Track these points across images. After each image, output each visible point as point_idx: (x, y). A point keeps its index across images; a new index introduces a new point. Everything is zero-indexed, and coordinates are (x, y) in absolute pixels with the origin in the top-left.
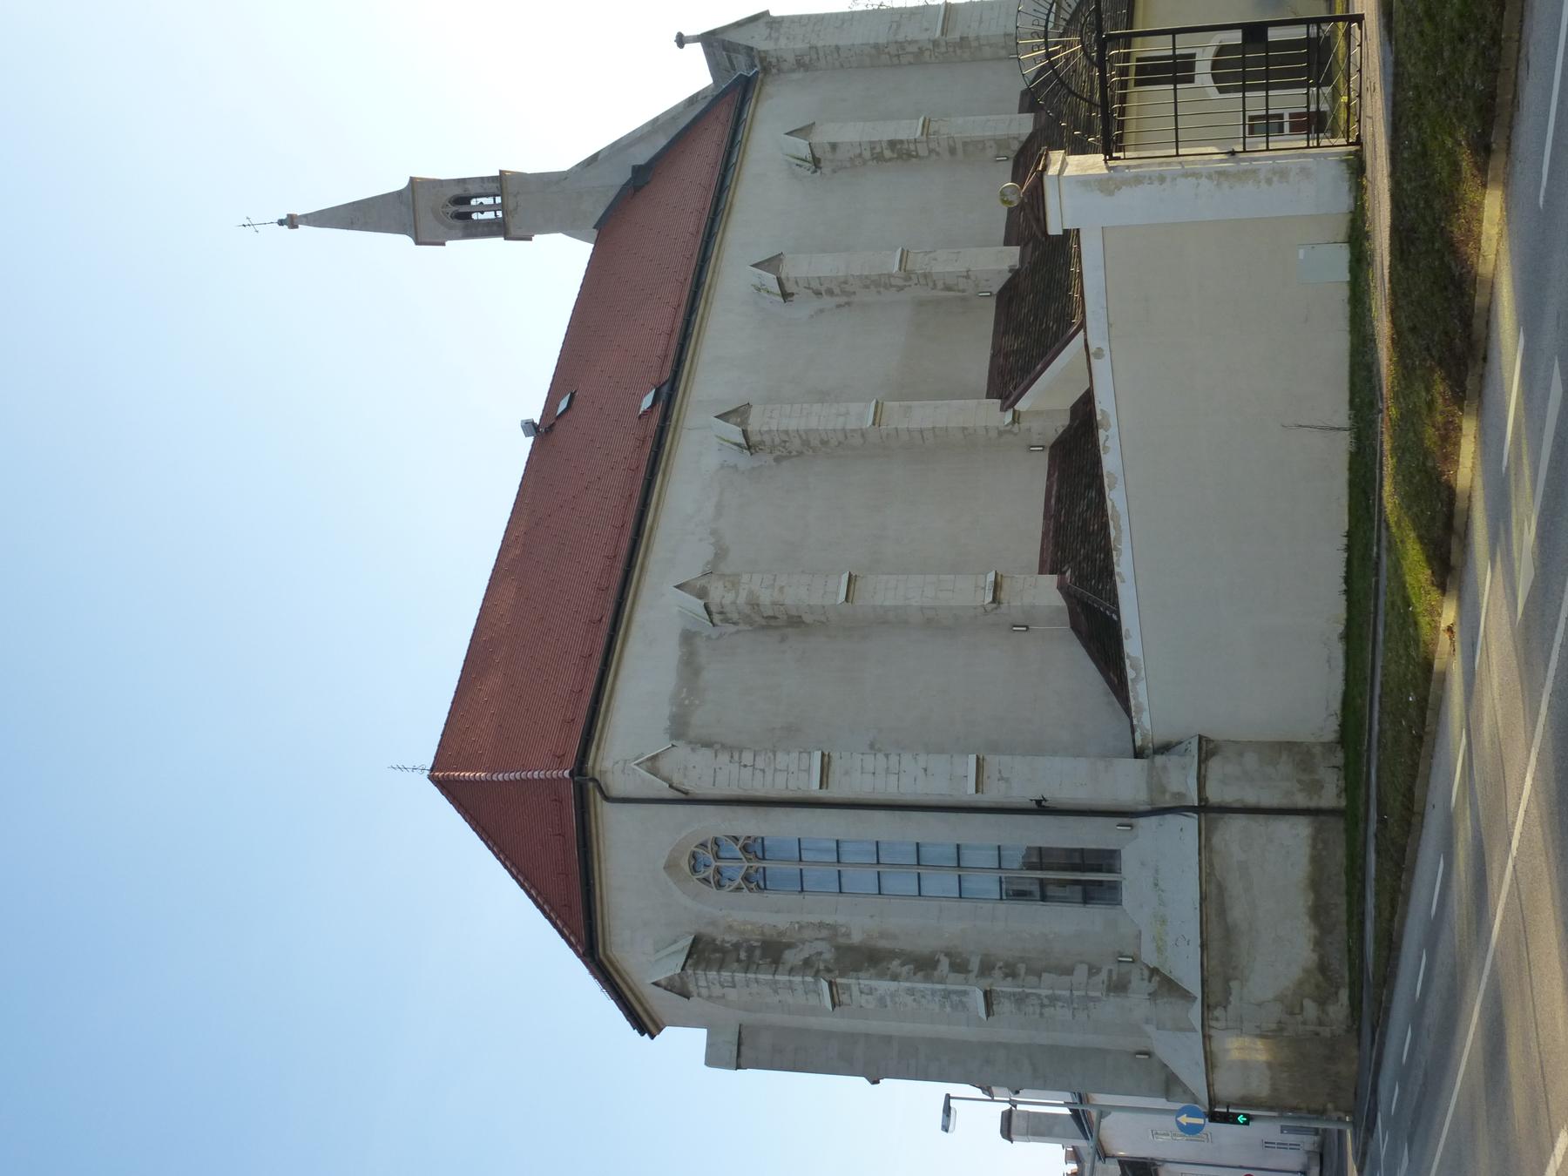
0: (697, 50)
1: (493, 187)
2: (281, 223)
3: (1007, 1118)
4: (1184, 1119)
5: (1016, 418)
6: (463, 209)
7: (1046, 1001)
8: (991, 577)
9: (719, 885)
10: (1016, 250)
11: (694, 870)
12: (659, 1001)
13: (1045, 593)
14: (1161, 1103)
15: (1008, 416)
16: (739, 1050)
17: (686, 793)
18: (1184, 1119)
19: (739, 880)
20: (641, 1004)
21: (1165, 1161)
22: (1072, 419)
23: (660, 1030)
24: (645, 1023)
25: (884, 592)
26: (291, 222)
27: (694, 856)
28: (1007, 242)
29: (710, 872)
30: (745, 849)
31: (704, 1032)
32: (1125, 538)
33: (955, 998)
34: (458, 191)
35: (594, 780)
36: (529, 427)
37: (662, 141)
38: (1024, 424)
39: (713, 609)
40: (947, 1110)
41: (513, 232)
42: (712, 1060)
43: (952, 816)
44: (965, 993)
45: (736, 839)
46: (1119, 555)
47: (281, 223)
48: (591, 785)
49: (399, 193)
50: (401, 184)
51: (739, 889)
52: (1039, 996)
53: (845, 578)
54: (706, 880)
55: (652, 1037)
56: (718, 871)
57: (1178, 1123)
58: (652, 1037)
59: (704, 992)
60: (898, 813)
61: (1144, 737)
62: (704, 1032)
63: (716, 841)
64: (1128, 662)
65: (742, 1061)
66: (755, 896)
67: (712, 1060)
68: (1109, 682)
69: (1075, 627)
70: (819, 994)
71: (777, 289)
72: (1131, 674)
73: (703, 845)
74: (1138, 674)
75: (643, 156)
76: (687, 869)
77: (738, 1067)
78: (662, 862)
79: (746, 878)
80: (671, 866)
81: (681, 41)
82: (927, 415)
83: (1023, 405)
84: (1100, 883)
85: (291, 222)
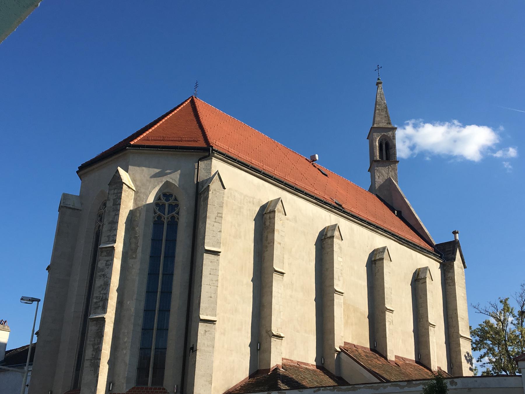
6: (384, 146)
7: (96, 347)
10: (393, 359)
11: (165, 195)
13: (276, 360)
15: (339, 350)
17: (201, 194)
20: (97, 168)
24: (84, 169)
27: (171, 195)
28: (396, 356)
30: (173, 217)
33: (101, 304)
34: (391, 144)
37: (412, 223)
39: (272, 215)
40: (33, 300)
42: (65, 197)
43: (185, 309)
45: (178, 213)
47: (378, 79)
48: (207, 154)
51: (155, 213)
55: (77, 172)
58: (77, 172)
59: (112, 191)
63: (177, 205)
67: (65, 197)
71: (377, 258)
73: (176, 199)
75: (404, 214)
77: (60, 207)
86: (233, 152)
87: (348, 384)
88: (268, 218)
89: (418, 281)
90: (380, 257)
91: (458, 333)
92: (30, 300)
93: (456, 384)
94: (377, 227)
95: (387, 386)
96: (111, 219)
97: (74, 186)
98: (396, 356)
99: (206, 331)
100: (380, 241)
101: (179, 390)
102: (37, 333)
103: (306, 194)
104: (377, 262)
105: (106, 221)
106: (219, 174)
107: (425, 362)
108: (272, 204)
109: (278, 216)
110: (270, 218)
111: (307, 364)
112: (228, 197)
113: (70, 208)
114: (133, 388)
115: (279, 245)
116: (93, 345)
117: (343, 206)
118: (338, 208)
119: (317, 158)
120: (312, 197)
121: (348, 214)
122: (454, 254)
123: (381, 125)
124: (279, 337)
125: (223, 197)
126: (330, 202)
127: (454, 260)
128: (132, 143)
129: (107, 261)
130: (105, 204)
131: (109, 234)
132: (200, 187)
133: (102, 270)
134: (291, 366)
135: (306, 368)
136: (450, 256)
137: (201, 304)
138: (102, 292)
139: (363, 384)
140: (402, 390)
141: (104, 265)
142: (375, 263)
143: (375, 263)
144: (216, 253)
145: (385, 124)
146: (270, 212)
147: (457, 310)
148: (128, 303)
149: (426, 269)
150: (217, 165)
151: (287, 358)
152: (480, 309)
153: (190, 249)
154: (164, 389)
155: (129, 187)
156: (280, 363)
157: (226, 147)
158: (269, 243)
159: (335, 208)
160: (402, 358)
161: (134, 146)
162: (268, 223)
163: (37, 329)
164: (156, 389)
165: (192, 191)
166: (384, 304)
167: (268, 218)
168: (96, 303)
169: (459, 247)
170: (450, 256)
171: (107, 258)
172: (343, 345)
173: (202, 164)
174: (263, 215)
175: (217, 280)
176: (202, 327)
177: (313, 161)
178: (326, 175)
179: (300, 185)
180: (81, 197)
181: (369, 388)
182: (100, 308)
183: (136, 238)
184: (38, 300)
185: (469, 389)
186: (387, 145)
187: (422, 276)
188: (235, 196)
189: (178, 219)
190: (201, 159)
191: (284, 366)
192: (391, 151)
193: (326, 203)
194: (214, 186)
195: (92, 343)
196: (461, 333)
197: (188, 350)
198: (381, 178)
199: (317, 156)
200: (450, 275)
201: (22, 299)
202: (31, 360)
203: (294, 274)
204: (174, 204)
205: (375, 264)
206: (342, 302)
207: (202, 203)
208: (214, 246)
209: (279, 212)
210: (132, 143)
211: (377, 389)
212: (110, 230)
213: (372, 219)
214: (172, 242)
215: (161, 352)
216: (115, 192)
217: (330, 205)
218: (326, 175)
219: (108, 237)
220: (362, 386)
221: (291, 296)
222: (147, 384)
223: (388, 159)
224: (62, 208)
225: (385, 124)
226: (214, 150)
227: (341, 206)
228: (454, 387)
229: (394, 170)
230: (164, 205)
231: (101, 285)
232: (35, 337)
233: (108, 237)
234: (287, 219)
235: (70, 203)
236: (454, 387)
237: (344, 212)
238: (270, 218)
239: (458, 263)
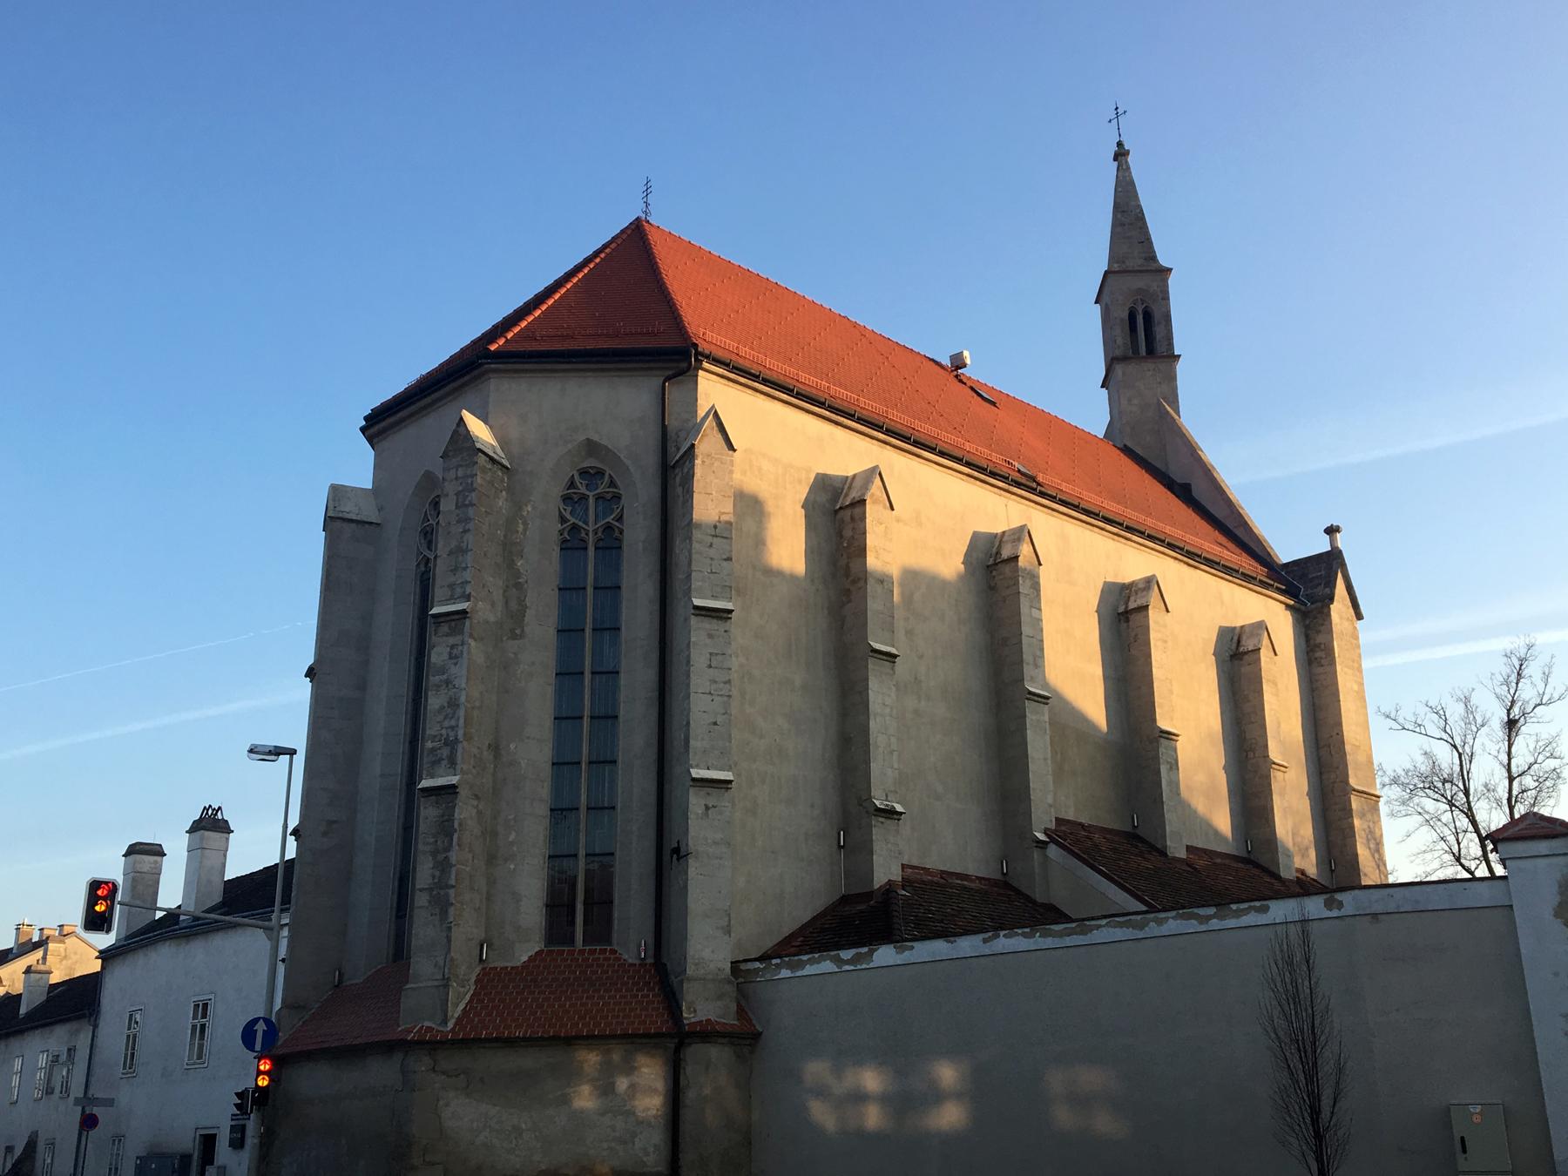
0: (1323, 546)
1: (1160, 348)
2: (1120, 144)
3: (157, 851)
4: (261, 1027)
5: (1042, 845)
7: (441, 857)
8: (899, 808)
9: (566, 499)
10: (1182, 854)
11: (584, 473)
12: (428, 432)
13: (885, 870)
14: (278, 1004)
15: (1041, 836)
16: (344, 525)
17: (673, 467)
18: (261, 1027)
19: (573, 520)
20: (411, 415)
21: (95, 1026)
22: (1043, 905)
23: (370, 440)
24: (379, 424)
25: (881, 694)
26: (1121, 154)
27: (601, 473)
29: (583, 490)
30: (608, 528)
31: (370, 487)
32: (1049, 942)
33: (445, 752)
34: (1157, 316)
35: (689, 368)
36: (958, 363)
38: (1036, 854)
39: (857, 510)
40: (278, 752)
41: (1119, 369)
42: (337, 493)
44: (452, 763)
45: (620, 519)
46: (1025, 935)
47: (1120, 144)
48: (685, 365)
49: (1154, 258)
50: (1164, 261)
51: (563, 520)
52: (448, 849)
53: (894, 651)
54: (572, 484)
55: (363, 430)
56: (584, 498)
57: (255, 1021)
58: (363, 430)
59: (452, 474)
60: (656, 694)
61: (757, 971)
62: (370, 487)
63: (617, 497)
64: (865, 950)
65: (338, 524)
66: (554, 537)
67: (337, 493)
68: (792, 936)
69: (844, 900)
70: (452, 599)
71: (1132, 605)
72: (846, 954)
73: (612, 484)
74: (848, 962)
76: (585, 465)
78: (596, 438)
79: (575, 528)
80: (592, 447)
81: (1331, 531)
82: (1038, 747)
83: (1053, 851)
84: (572, 923)
85: (1121, 154)
86: (748, 354)
87: (1069, 920)
88: (847, 518)
89: (1237, 656)
90: (1140, 602)
91: (1347, 783)
92: (270, 753)
93: (1340, 905)
94: (1129, 529)
95: (1167, 919)
96: (454, 544)
97: (357, 466)
98: (1188, 847)
99: (707, 808)
100: (1135, 562)
101: (651, 952)
102: (295, 832)
103: (942, 454)
104: (1132, 617)
105: (442, 547)
106: (716, 415)
107: (1264, 860)
108: (857, 484)
109: (874, 513)
110: (852, 519)
111: (965, 877)
112: (744, 473)
113: (351, 521)
114: (539, 953)
115: (879, 588)
116: (434, 854)
117: (1040, 479)
118: (1027, 485)
119: (968, 361)
120: (958, 460)
121: (1052, 498)
122: (1331, 584)
123: (1130, 264)
124: (890, 813)
125: (731, 472)
126: (1004, 471)
127: (1331, 599)
128: (493, 347)
129: (452, 647)
130: (436, 504)
131: (452, 579)
132: (671, 449)
133: (442, 671)
134: (923, 882)
135: (965, 888)
136: (1321, 591)
137: (692, 742)
138: (446, 724)
139: (1105, 917)
140: (1203, 928)
141: (446, 656)
142: (1125, 616)
143: (1125, 616)
144: (722, 615)
145: (1140, 262)
146: (853, 505)
147: (1340, 724)
148: (512, 746)
149: (1261, 626)
150: (712, 390)
151: (915, 862)
152: (1401, 720)
153: (657, 607)
154: (613, 952)
155: (491, 459)
156: (896, 875)
157: (732, 344)
158: (854, 582)
159: (1018, 485)
160: (1205, 851)
161: (500, 356)
162: (848, 533)
163: (294, 822)
164: (592, 952)
165: (651, 461)
166: (1154, 720)
167: (847, 518)
168: (433, 750)
169: (1343, 565)
170: (1321, 591)
171: (452, 640)
172: (1053, 826)
173: (674, 393)
174: (836, 512)
175: (729, 682)
176: (696, 802)
177: (958, 368)
178: (994, 404)
179: (925, 429)
180: (376, 490)
181: (1121, 925)
182: (444, 762)
183: (518, 586)
184: (292, 752)
185: (1375, 916)
186: (1148, 316)
187: (1249, 644)
188: (760, 469)
189: (621, 532)
190: (668, 379)
191: (906, 883)
192: (1159, 332)
193: (993, 475)
194: (706, 444)
195: (428, 848)
196: (1353, 782)
197: (666, 857)
198: (1135, 401)
199: (966, 353)
200: (1320, 639)
201: (251, 751)
202: (286, 900)
203: (921, 657)
204: (609, 496)
205: (1127, 620)
206: (1046, 718)
207: (679, 490)
208: (714, 597)
209: (876, 502)
210: (493, 347)
211: (1141, 927)
212: (454, 571)
213: (1111, 507)
214: (610, 590)
215: (603, 864)
216: (460, 473)
217: (1004, 478)
218: (994, 404)
219: (451, 586)
220: (1104, 922)
221: (916, 712)
222: (572, 941)
223: (1151, 351)
224: (333, 522)
225: (1140, 262)
226: (702, 354)
227: (1034, 479)
228: (1335, 913)
229: (1171, 378)
230: (584, 498)
231: (443, 707)
232: (292, 843)
233: (451, 586)
234: (898, 520)
235: (349, 509)
236: (1335, 913)
237: (1042, 495)
238: (852, 519)
239: (1339, 609)
